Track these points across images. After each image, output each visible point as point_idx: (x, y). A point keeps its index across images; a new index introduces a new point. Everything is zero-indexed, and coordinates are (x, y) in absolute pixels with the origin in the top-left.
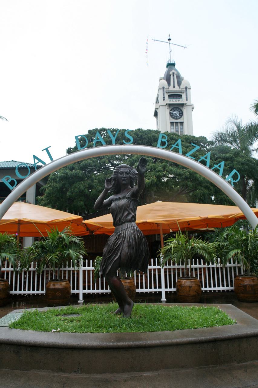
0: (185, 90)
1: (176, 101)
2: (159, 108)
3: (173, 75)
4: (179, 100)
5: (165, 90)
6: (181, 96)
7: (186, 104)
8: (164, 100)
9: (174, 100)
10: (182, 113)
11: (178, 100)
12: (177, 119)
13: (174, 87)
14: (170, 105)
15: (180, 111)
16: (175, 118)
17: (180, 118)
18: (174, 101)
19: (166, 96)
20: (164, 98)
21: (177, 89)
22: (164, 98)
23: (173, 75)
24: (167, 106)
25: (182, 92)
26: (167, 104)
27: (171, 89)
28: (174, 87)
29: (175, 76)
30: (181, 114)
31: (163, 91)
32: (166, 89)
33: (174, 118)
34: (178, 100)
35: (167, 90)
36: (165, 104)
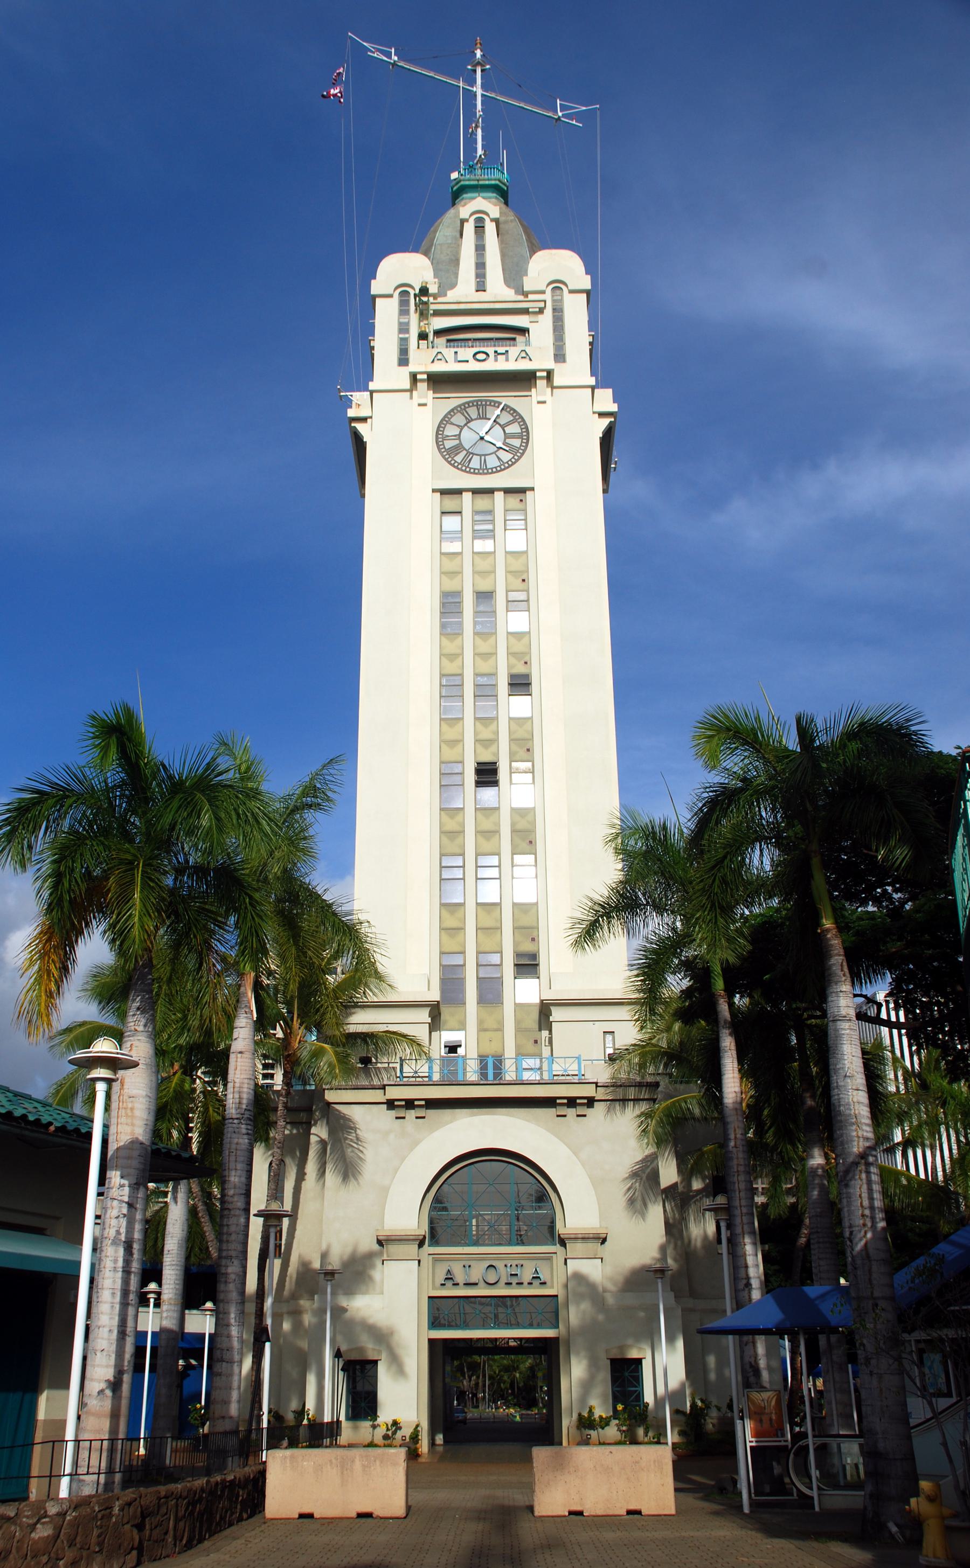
0: (548, 296)
1: (480, 356)
3: (480, 228)
4: (501, 350)
7: (549, 375)
8: (403, 360)
9: (466, 353)
10: (525, 434)
11: (490, 351)
12: (484, 471)
14: (439, 381)
15: (508, 424)
16: (475, 463)
17: (503, 467)
23: (480, 228)
25: (525, 311)
29: (490, 228)
33: (464, 467)
34: (496, 352)
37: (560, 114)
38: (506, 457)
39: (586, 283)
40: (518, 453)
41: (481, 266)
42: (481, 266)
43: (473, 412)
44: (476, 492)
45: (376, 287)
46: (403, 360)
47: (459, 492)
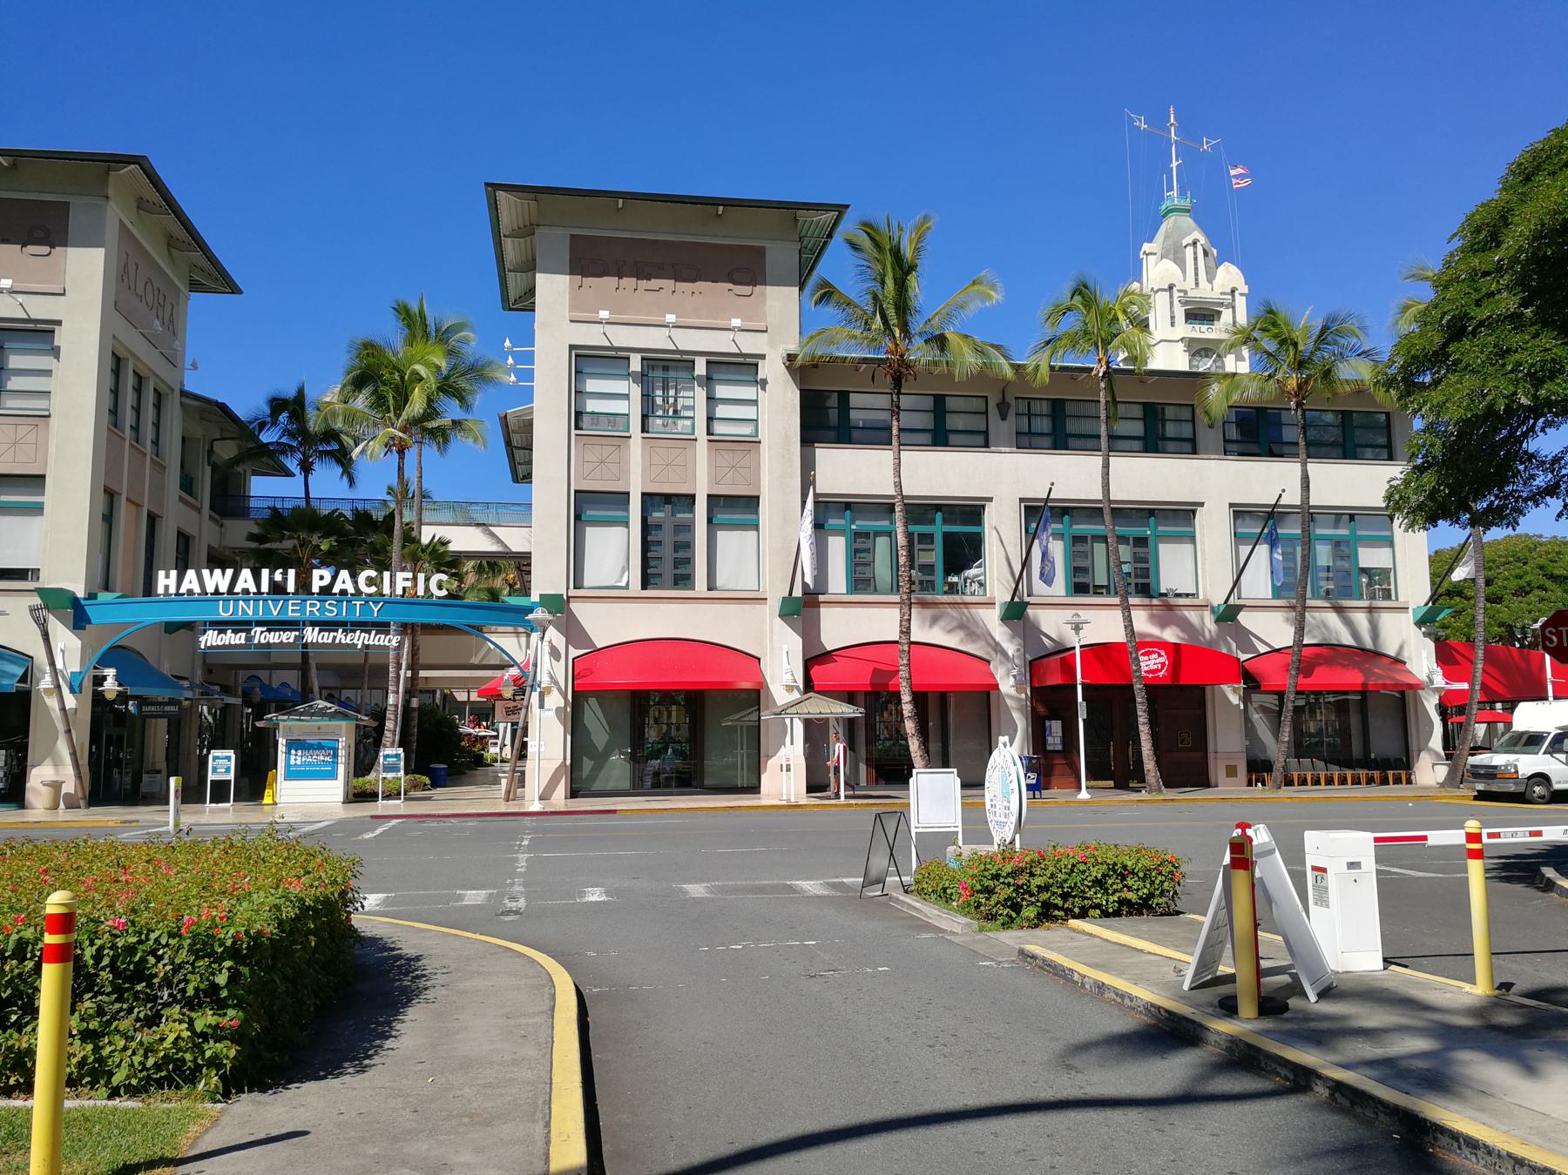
5: (1176, 294)
8: (1173, 324)
13: (1197, 284)
18: (1202, 332)
19: (1180, 313)
21: (1207, 292)
31: (1171, 297)
32: (1179, 291)
39: (1245, 289)
41: (1196, 269)
46: (1173, 324)
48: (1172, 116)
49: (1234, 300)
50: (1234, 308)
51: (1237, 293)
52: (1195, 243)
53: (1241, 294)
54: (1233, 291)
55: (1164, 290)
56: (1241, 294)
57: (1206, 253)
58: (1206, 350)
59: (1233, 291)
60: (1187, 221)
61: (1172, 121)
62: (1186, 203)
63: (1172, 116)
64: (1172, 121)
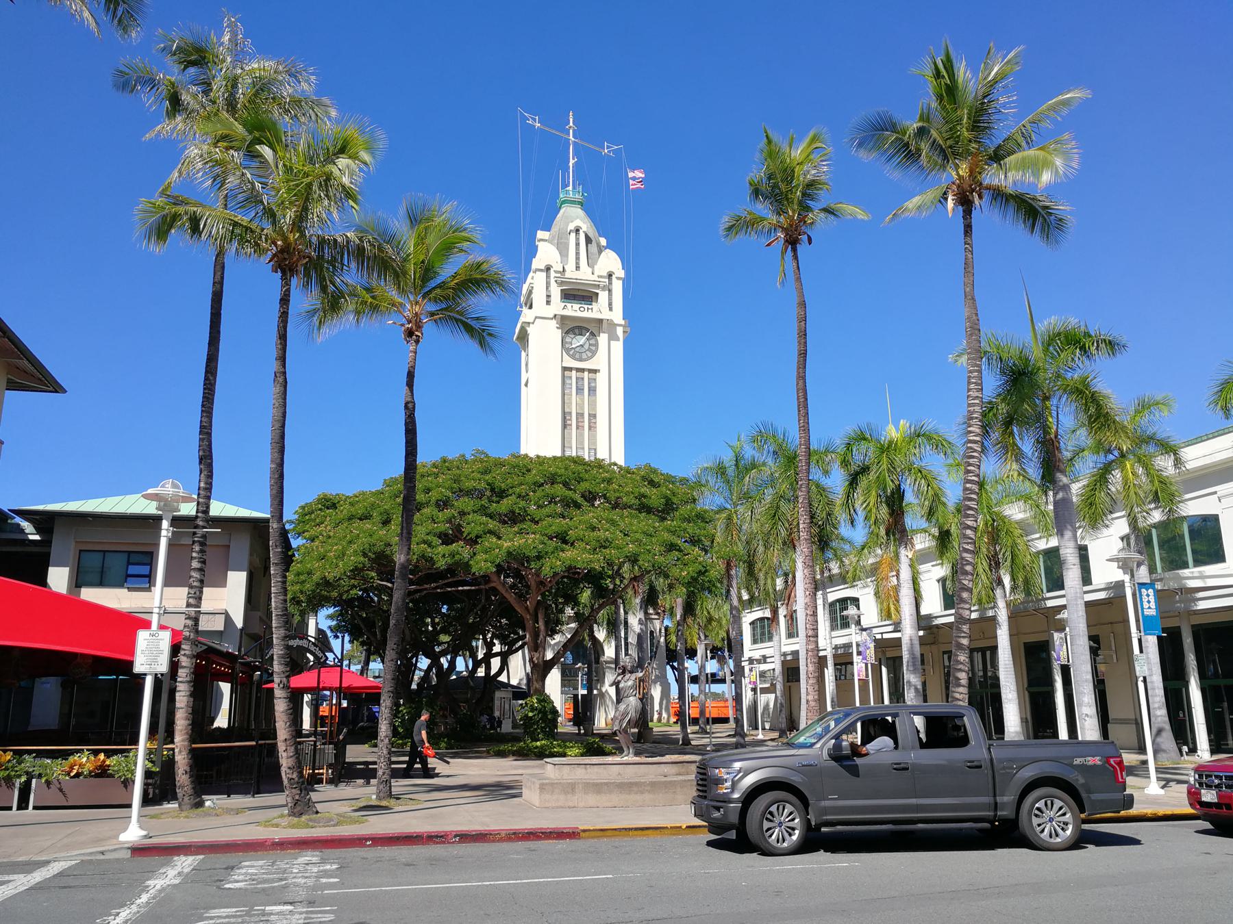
1: (582, 309)
2: (533, 323)
4: (590, 307)
5: (553, 274)
6: (597, 294)
8: (548, 303)
9: (576, 306)
10: (596, 345)
11: (586, 306)
12: (581, 360)
13: (578, 268)
16: (577, 356)
18: (574, 310)
19: (556, 292)
20: (549, 296)
21: (585, 275)
22: (549, 296)
24: (554, 322)
26: (555, 316)
27: (571, 273)
28: (578, 268)
30: (593, 348)
31: (548, 277)
32: (556, 272)
33: (573, 357)
35: (559, 275)
36: (552, 316)
37: (606, 151)
38: (590, 354)
39: (622, 274)
40: (594, 353)
41: (577, 254)
42: (577, 254)
43: (577, 331)
44: (578, 370)
45: (537, 263)
46: (548, 303)
47: (570, 369)
48: (571, 120)
49: (610, 283)
50: (610, 291)
51: (614, 277)
52: (577, 231)
53: (618, 278)
54: (610, 275)
55: (541, 270)
56: (618, 278)
57: (588, 240)
58: (580, 328)
59: (610, 275)
60: (578, 211)
61: (571, 124)
62: (578, 197)
63: (571, 120)
64: (571, 124)
